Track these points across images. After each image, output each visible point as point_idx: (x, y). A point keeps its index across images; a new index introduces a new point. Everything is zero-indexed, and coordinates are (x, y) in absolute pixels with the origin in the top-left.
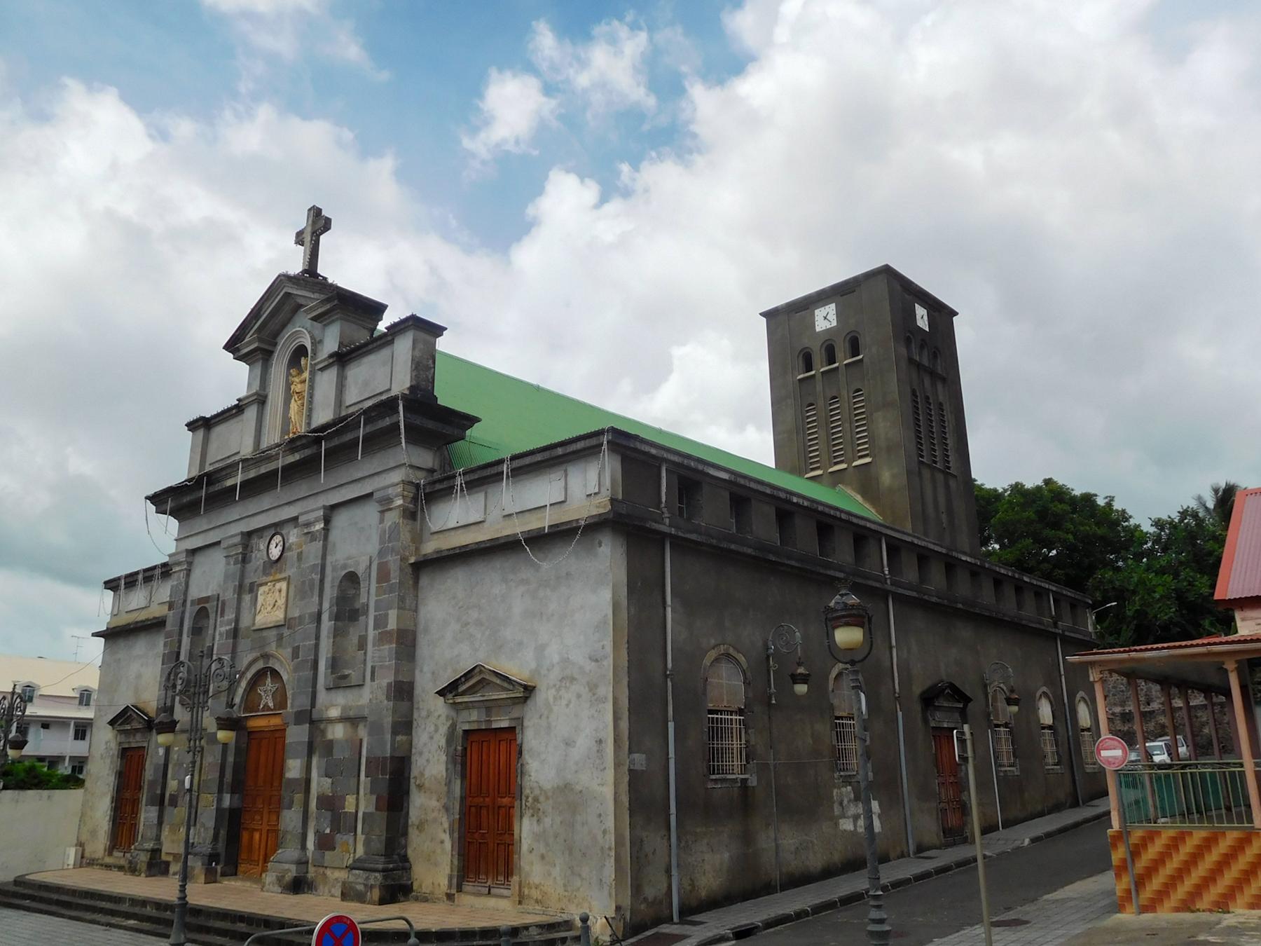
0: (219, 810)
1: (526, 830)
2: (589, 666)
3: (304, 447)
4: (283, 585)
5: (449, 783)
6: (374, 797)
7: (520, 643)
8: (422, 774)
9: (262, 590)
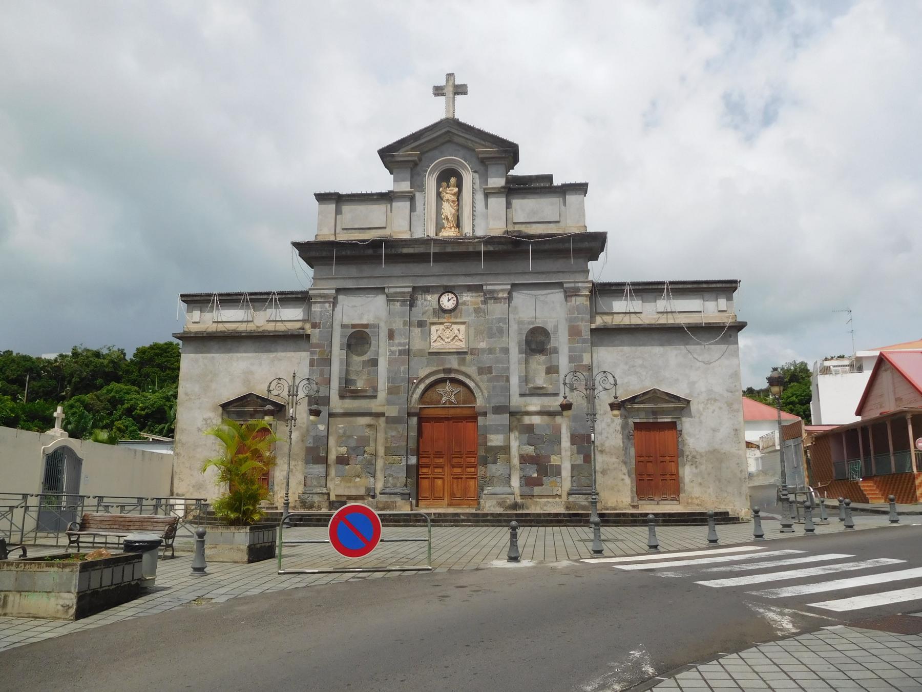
0: (408, 467)
1: (687, 473)
2: (726, 394)
3: (499, 243)
4: (462, 327)
5: (625, 449)
7: (677, 380)
8: (602, 445)
9: (433, 328)
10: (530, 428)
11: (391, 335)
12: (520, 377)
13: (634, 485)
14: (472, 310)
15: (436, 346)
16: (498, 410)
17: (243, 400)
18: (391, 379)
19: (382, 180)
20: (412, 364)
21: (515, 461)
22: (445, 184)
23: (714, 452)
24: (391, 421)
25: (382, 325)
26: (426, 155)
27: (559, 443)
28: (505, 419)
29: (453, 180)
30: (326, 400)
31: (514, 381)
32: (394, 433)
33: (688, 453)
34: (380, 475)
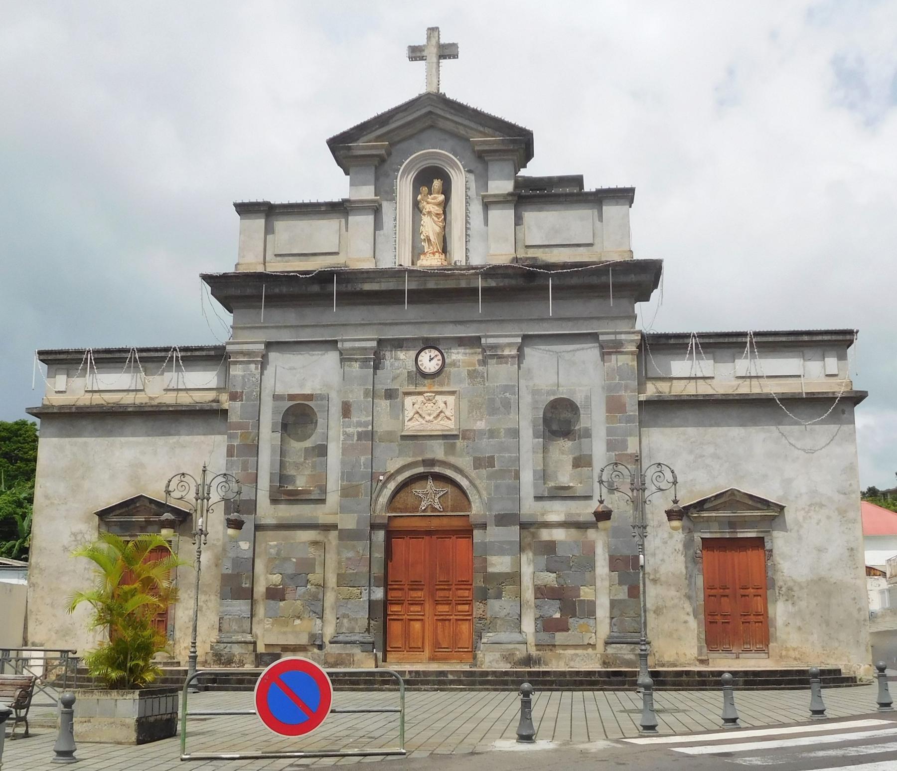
1: (780, 611)
3: (506, 276)
4: (451, 399)
5: (690, 577)
6: (626, 588)
7: (765, 476)
8: (656, 571)
9: (408, 401)
10: (550, 547)
11: (346, 410)
12: (535, 472)
13: (703, 629)
14: (465, 374)
15: (412, 426)
16: (503, 520)
17: (129, 506)
18: (346, 475)
19: (335, 184)
20: (377, 453)
21: (528, 594)
22: (425, 189)
23: (820, 580)
24: (346, 536)
25: (333, 395)
26: (399, 146)
27: (593, 568)
28: (513, 533)
29: (437, 184)
30: (251, 506)
31: (527, 477)
32: (350, 554)
33: (780, 583)
34: (329, 616)
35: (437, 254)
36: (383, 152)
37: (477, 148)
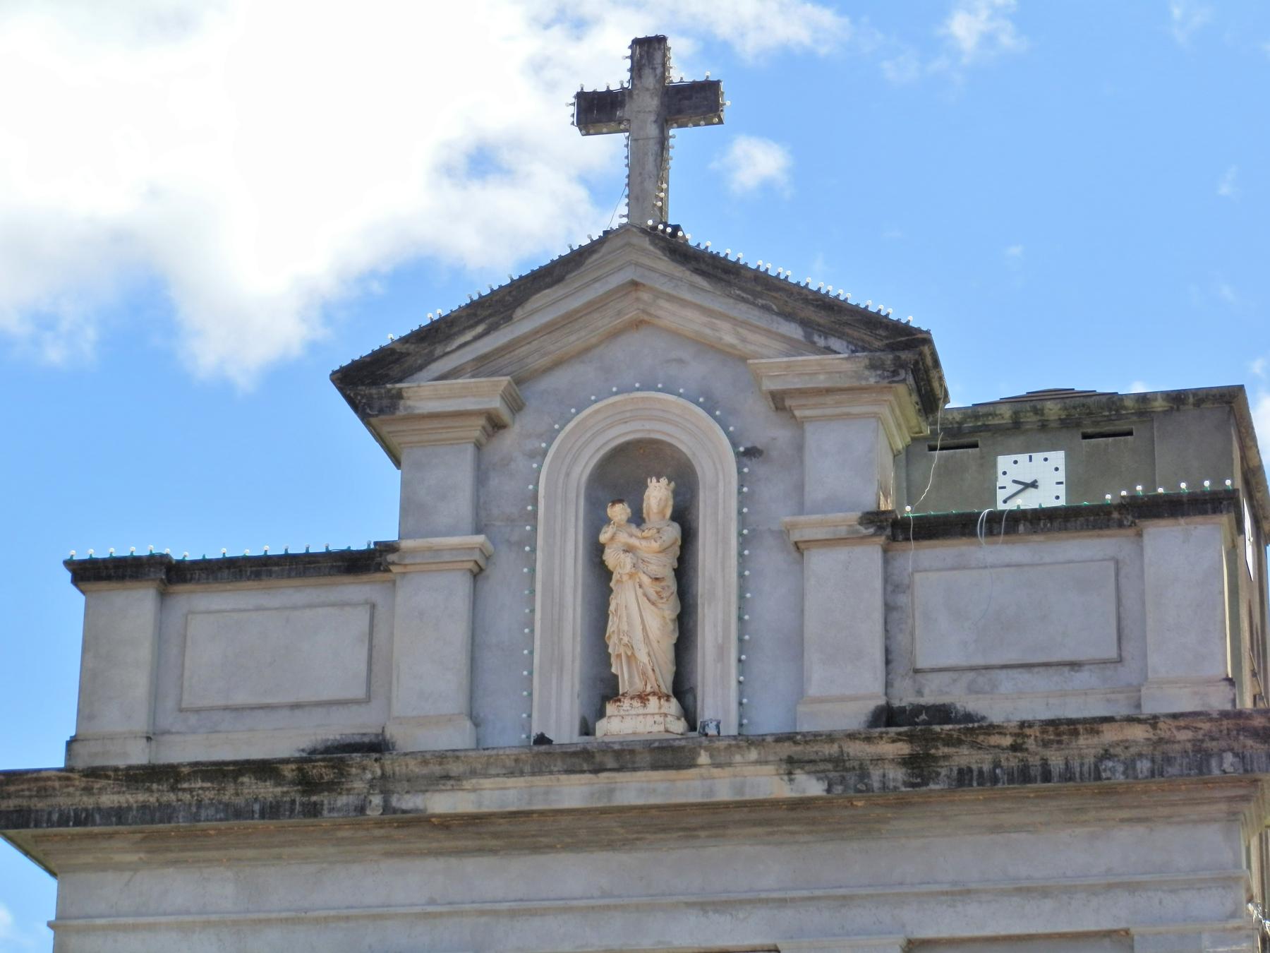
22: (619, 512)
26: (547, 383)
29: (658, 494)
35: (653, 701)
36: (496, 404)
37: (770, 385)
